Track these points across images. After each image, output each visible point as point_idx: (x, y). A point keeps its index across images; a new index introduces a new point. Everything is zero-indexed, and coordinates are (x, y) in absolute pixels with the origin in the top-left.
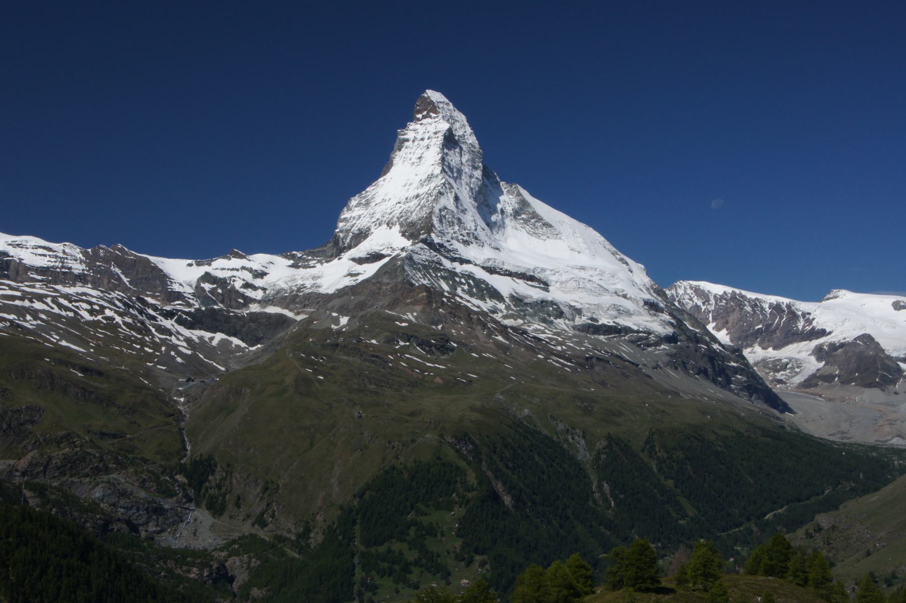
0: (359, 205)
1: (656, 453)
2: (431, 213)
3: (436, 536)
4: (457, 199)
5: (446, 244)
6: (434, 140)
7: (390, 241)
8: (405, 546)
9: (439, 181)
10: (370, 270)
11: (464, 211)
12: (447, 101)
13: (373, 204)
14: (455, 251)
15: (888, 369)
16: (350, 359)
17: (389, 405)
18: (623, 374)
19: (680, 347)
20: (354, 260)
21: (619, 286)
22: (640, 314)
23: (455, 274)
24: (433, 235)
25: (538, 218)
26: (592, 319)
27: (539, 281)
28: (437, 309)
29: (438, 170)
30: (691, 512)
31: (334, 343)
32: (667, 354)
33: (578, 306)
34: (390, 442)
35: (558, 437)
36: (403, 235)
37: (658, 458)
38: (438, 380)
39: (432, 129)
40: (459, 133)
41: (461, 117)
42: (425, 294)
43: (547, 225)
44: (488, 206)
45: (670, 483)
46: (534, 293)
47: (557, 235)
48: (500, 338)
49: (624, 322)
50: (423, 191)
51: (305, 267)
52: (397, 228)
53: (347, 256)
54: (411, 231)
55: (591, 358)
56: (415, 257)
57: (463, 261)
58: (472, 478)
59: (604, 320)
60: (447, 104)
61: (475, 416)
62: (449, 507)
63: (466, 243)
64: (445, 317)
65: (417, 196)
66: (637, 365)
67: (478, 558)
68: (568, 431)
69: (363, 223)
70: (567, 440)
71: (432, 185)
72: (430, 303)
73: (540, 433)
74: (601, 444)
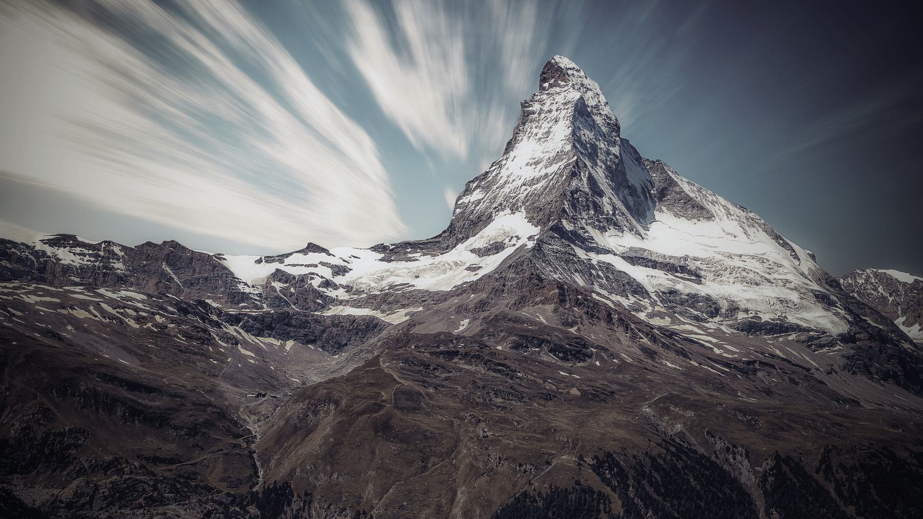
1: (833, 475)
4: (591, 179)
5: (581, 232)
6: (564, 112)
10: (491, 263)
11: (601, 194)
12: (576, 67)
16: (473, 368)
18: (791, 380)
19: (860, 348)
20: (473, 251)
23: (592, 267)
24: (564, 222)
27: (690, 272)
29: (568, 148)
32: (843, 356)
34: (521, 465)
35: (717, 457)
37: (836, 481)
38: (575, 391)
39: (560, 99)
42: (557, 291)
46: (685, 287)
47: (710, 217)
48: (645, 340)
50: (550, 170)
55: (755, 361)
57: (599, 251)
60: (578, 71)
61: (621, 433)
64: (581, 317)
65: (546, 175)
66: (808, 370)
68: (728, 449)
70: (727, 460)
72: (562, 301)
73: (695, 452)
74: (767, 465)
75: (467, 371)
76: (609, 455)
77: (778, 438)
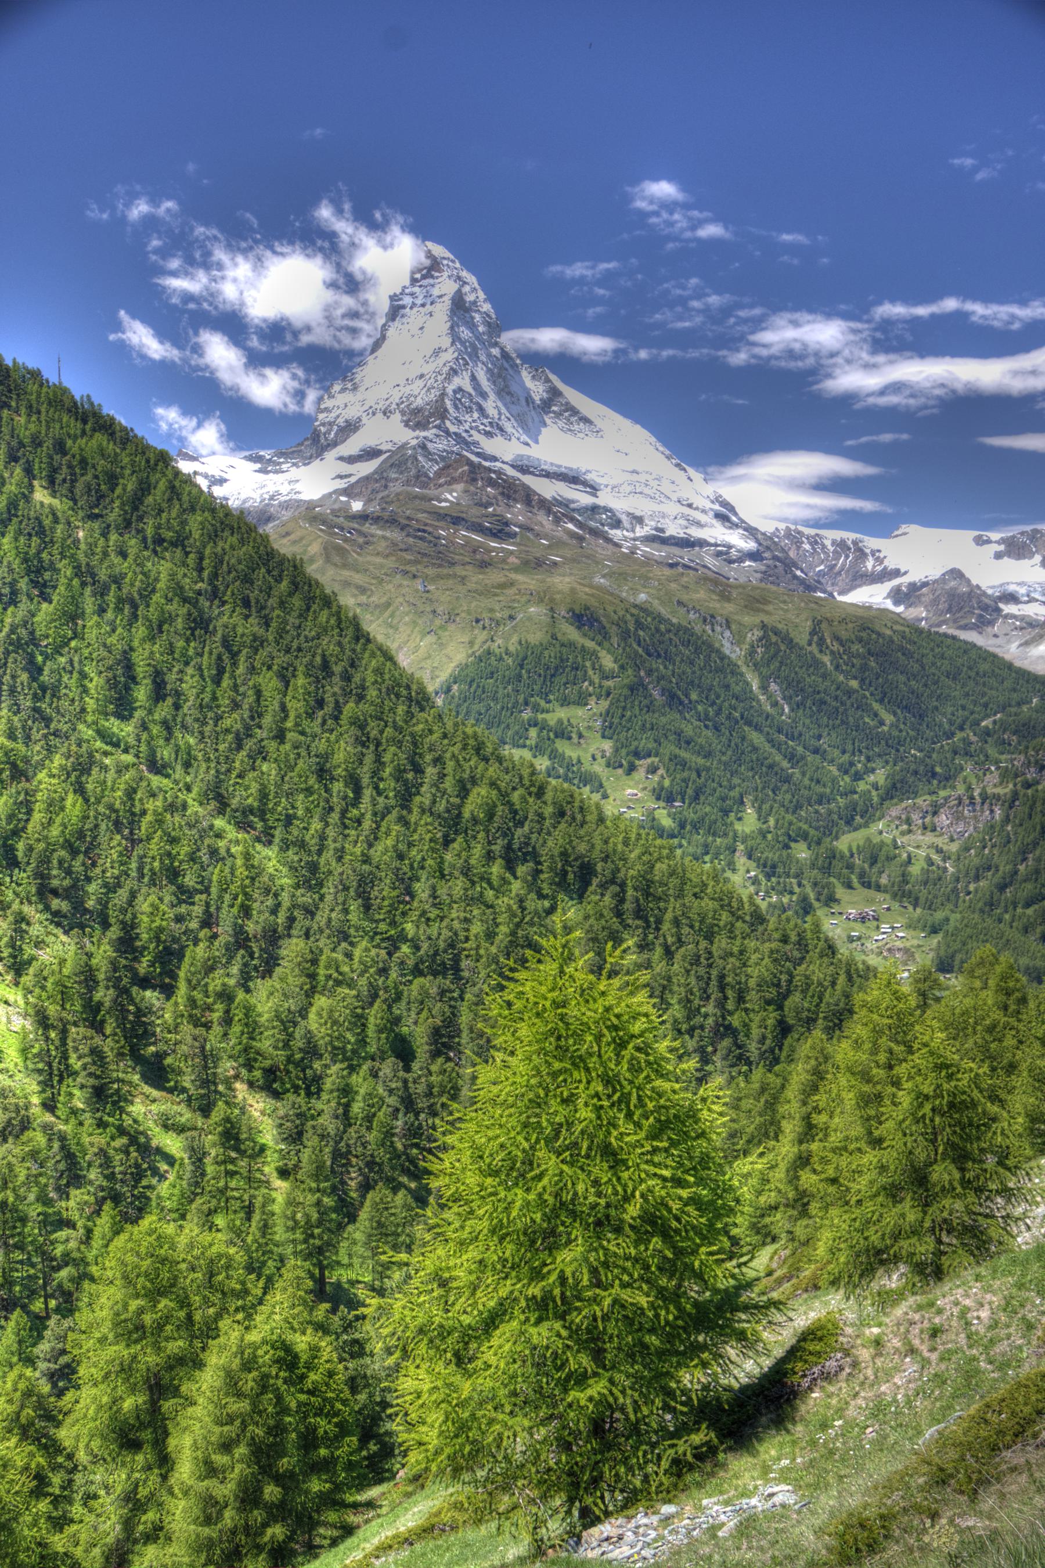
0: (343, 390)
2: (443, 395)
3: (570, 738)
4: (473, 378)
7: (391, 433)
8: (527, 754)
9: (449, 356)
10: (367, 468)
13: (362, 389)
14: (476, 444)
15: (985, 608)
16: (388, 534)
17: (463, 578)
20: (341, 458)
21: (684, 495)
24: (448, 423)
25: (574, 411)
26: (657, 529)
27: (585, 483)
29: (446, 341)
30: (889, 718)
31: (363, 517)
33: (638, 513)
36: (407, 425)
37: (832, 653)
38: (513, 560)
40: (470, 298)
41: (471, 279)
43: (586, 420)
44: (509, 393)
45: (854, 684)
48: (570, 526)
49: (696, 533)
51: (276, 472)
52: (397, 417)
53: (331, 455)
54: (416, 418)
56: (429, 445)
58: (608, 662)
59: (673, 530)
62: (581, 701)
63: (489, 434)
65: (422, 376)
67: (643, 764)
71: (440, 361)
72: (474, 480)
75: (384, 537)
76: (587, 608)
77: (758, 610)
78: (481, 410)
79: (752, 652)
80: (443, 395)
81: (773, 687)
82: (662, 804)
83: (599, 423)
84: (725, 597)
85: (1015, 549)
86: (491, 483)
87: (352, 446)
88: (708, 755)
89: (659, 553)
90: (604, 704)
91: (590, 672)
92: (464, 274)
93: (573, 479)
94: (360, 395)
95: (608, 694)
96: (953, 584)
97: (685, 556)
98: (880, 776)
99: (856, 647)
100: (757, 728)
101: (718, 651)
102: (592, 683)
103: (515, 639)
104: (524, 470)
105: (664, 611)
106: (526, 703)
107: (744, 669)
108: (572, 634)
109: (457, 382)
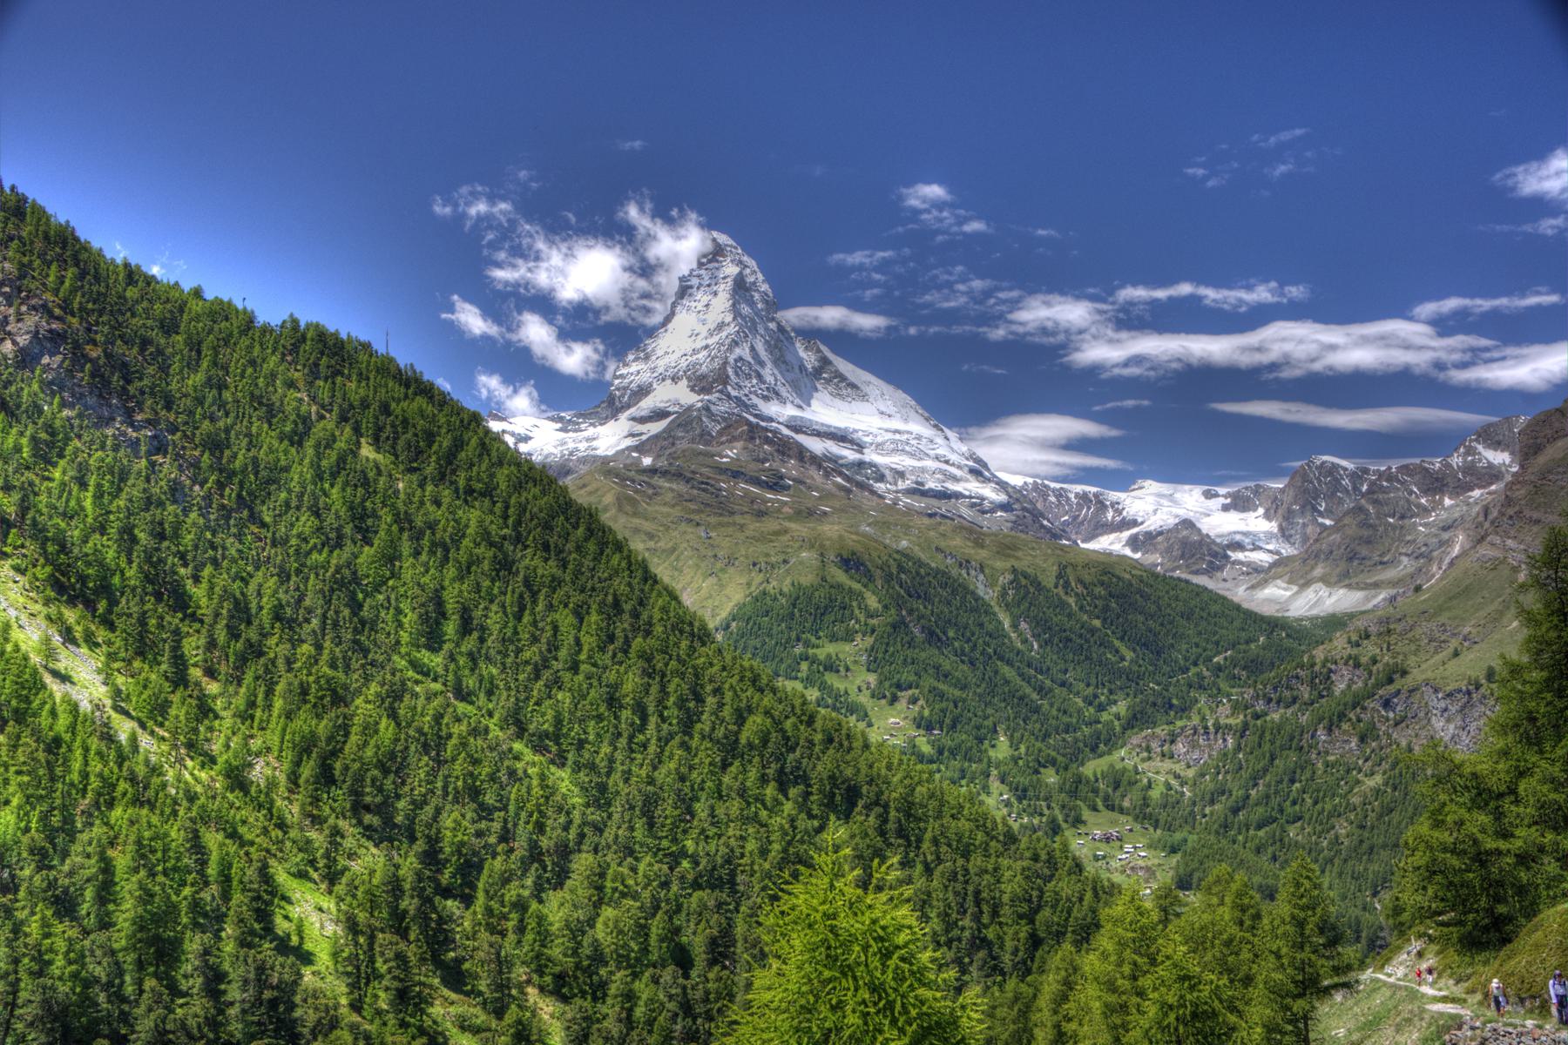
0: (636, 359)
2: (726, 363)
3: (838, 671)
4: (753, 349)
7: (681, 395)
8: (798, 686)
9: (732, 329)
10: (656, 427)
11: (762, 364)
14: (755, 406)
15: (1215, 555)
16: (674, 486)
20: (633, 419)
21: (940, 451)
22: (967, 481)
25: (843, 378)
26: (917, 483)
27: (852, 442)
28: (760, 446)
29: (729, 318)
30: (1129, 655)
31: (652, 471)
36: (692, 390)
43: (853, 386)
45: (1097, 623)
46: (850, 455)
47: (864, 397)
48: (839, 480)
49: (953, 487)
50: (710, 341)
52: (685, 382)
54: (701, 383)
56: (713, 408)
58: (873, 602)
59: (931, 484)
62: (849, 637)
63: (766, 398)
65: (707, 347)
67: (905, 695)
69: (645, 377)
71: (724, 334)
72: (752, 438)
75: (672, 490)
76: (854, 553)
77: (1009, 556)
78: (759, 376)
79: (1004, 594)
80: (726, 363)
81: (1023, 626)
82: (922, 732)
83: (867, 389)
84: (978, 543)
85: (1239, 503)
86: (768, 441)
87: (646, 405)
88: (964, 688)
89: (919, 504)
90: (869, 640)
91: (857, 611)
92: (745, 258)
93: (841, 437)
94: (651, 364)
95: (873, 631)
96: (1185, 533)
97: (943, 507)
98: (1121, 707)
99: (1099, 590)
100: (1009, 663)
101: (973, 593)
102: (858, 621)
103: (788, 581)
104: (797, 429)
105: (923, 557)
106: (798, 639)
107: (996, 609)
108: (840, 576)
109: (738, 351)
